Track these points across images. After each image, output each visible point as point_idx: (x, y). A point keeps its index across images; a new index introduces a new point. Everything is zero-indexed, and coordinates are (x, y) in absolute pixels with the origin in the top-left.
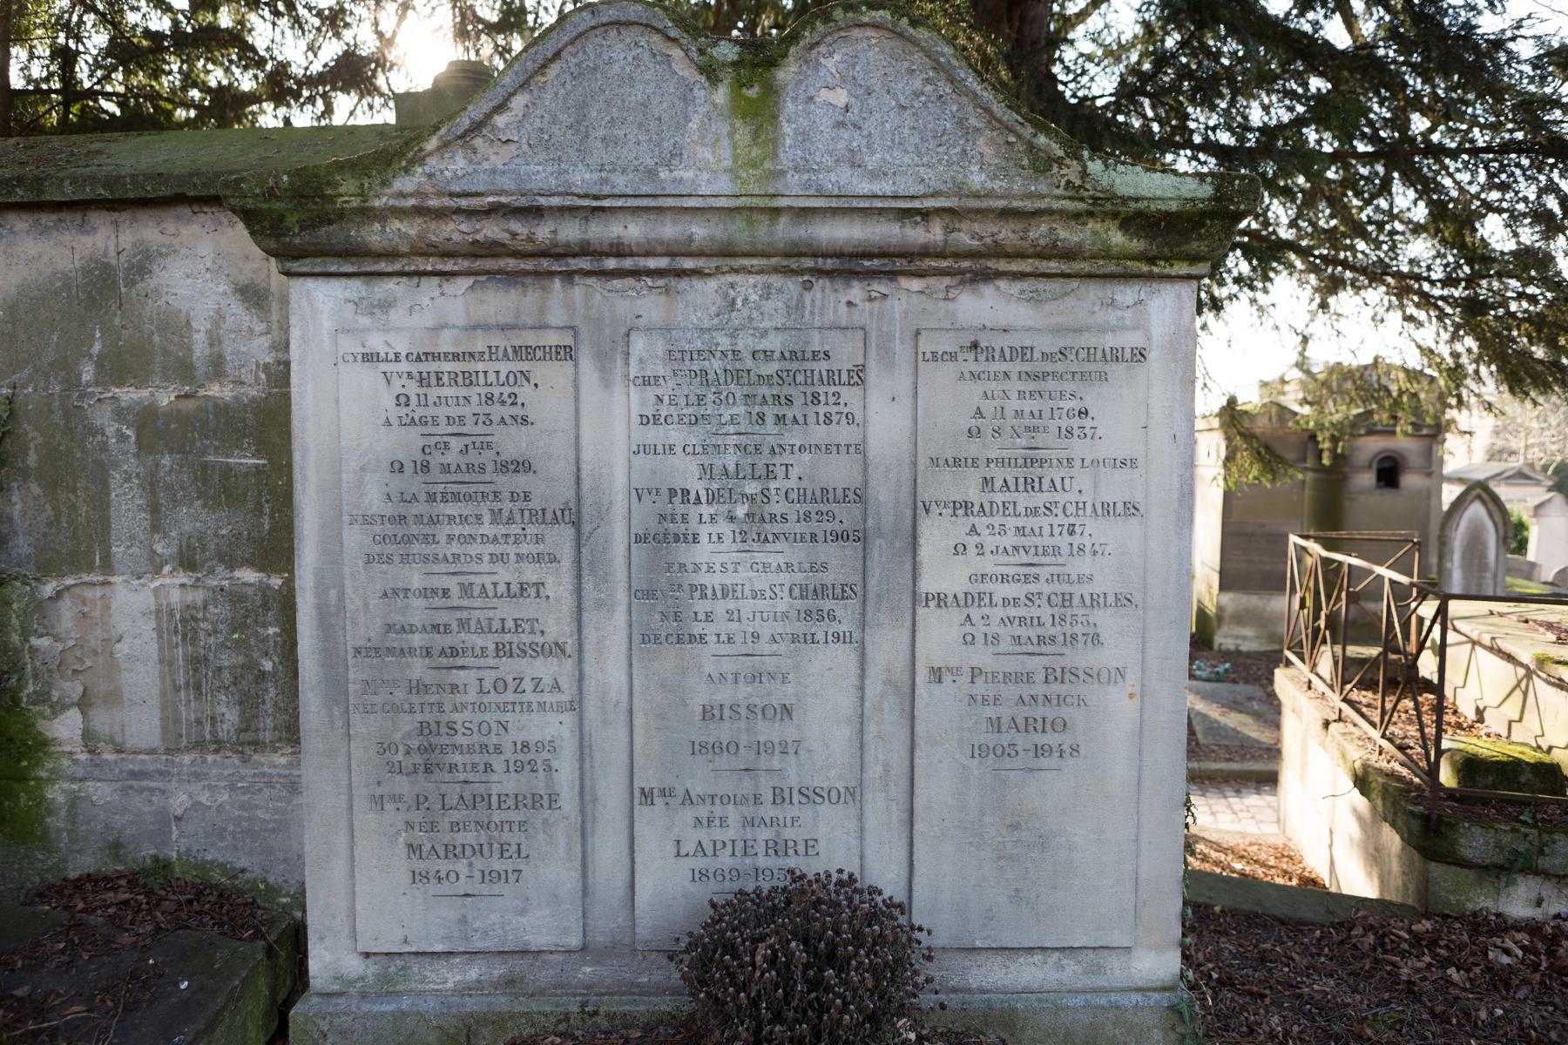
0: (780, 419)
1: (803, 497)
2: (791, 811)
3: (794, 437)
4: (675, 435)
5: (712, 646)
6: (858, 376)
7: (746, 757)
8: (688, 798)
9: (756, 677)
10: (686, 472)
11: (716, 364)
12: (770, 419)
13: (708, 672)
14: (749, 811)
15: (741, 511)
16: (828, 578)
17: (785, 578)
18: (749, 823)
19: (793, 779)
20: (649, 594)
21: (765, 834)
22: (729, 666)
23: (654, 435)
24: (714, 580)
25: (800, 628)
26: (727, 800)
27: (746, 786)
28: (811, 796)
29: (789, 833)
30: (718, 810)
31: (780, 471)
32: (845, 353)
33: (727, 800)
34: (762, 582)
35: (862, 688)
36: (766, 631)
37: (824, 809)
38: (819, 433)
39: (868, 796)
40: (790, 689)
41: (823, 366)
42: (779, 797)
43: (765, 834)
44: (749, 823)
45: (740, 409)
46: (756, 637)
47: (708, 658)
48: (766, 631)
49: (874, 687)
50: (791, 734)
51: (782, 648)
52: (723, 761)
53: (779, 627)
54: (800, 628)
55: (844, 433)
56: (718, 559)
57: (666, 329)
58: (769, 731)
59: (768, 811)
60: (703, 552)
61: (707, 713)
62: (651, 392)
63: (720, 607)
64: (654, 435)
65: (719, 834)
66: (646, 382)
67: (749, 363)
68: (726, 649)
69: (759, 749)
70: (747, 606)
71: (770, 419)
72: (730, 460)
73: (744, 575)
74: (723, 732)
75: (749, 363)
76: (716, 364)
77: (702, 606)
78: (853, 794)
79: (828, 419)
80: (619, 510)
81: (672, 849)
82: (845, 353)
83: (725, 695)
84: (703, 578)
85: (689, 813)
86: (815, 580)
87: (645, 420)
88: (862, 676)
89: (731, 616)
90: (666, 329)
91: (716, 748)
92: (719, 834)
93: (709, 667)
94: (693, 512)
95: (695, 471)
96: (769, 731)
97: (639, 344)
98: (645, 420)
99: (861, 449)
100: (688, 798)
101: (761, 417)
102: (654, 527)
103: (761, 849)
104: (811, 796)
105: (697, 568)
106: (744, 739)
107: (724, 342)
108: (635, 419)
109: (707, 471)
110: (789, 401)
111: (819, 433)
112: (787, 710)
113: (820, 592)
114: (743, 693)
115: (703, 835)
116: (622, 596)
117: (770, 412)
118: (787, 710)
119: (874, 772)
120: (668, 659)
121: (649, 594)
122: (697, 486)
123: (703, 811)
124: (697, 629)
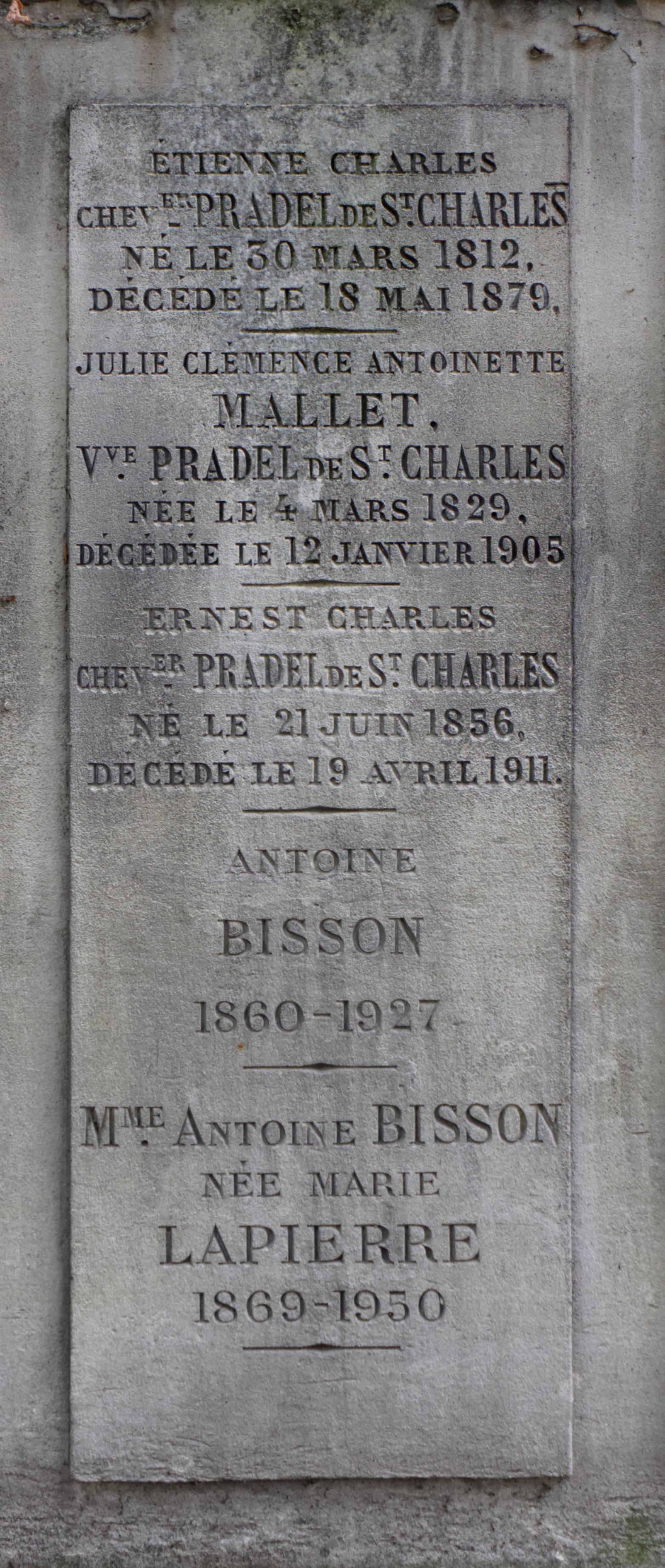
0: (390, 298)
1: (439, 464)
2: (416, 1159)
3: (422, 336)
4: (168, 331)
5: (247, 791)
6: (554, 206)
7: (320, 1036)
8: (191, 1130)
9: (341, 857)
10: (191, 408)
11: (251, 183)
12: (369, 297)
13: (233, 849)
14: (326, 1157)
15: (308, 494)
16: (496, 640)
17: (402, 638)
18: (326, 1184)
19: (423, 1088)
20: (109, 674)
21: (358, 1211)
22: (281, 833)
23: (122, 331)
24: (253, 644)
25: (434, 748)
26: (274, 1133)
27: (320, 1105)
28: (464, 1123)
29: (415, 1209)
30: (257, 1160)
31: (390, 409)
32: (526, 168)
33: (274, 1133)
34: (352, 648)
35: (568, 883)
36: (362, 754)
37: (492, 1150)
38: (475, 328)
39: (586, 1122)
40: (412, 884)
41: (480, 185)
42: (394, 1124)
43: (358, 1211)
44: (326, 1184)
45: (304, 278)
46: (341, 768)
47: (237, 817)
48: (362, 754)
49: (595, 879)
50: (418, 984)
51: (397, 793)
52: (269, 1045)
53: (392, 748)
54: (434, 748)
55: (524, 328)
56: (260, 599)
57: (149, 109)
58: (369, 978)
59: (370, 1157)
60: (226, 583)
61: (234, 938)
62: (114, 241)
63: (266, 701)
64: (122, 331)
65: (256, 1211)
66: (106, 218)
67: (324, 180)
68: (274, 795)
69: (350, 1016)
70: (320, 700)
71: (369, 297)
72: (285, 386)
73: (313, 633)
74: (269, 979)
75: (324, 180)
76: (251, 183)
77: (223, 702)
78: (551, 1120)
79: (493, 298)
80: (42, 496)
81: (154, 1247)
82: (527, 160)
83: (271, 896)
84: (227, 641)
85: (192, 1165)
86: (462, 644)
87: (102, 300)
88: (570, 857)
89: (288, 722)
90: (149, 109)
91: (251, 1017)
92: (256, 1211)
93: (236, 840)
94: (205, 496)
95: (212, 409)
96: (369, 978)
97: (88, 139)
98: (102, 300)
99: (560, 361)
100: (191, 1130)
101: (351, 292)
102: (119, 528)
103: (352, 1245)
104: (464, 1123)
105: (213, 615)
106: (313, 996)
107: (272, 136)
108: (80, 297)
109: (233, 408)
110: (410, 259)
111: (475, 328)
112: (409, 932)
113: (479, 669)
114: (313, 892)
115: (227, 1216)
116: (47, 679)
117: (370, 283)
118: (409, 932)
119: (598, 1068)
120: (147, 819)
121: (109, 674)
122: (213, 441)
123: (225, 1158)
124: (213, 751)
